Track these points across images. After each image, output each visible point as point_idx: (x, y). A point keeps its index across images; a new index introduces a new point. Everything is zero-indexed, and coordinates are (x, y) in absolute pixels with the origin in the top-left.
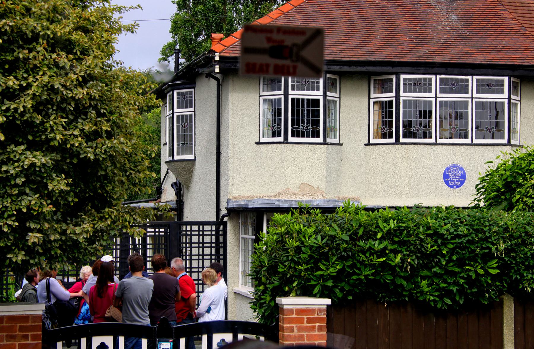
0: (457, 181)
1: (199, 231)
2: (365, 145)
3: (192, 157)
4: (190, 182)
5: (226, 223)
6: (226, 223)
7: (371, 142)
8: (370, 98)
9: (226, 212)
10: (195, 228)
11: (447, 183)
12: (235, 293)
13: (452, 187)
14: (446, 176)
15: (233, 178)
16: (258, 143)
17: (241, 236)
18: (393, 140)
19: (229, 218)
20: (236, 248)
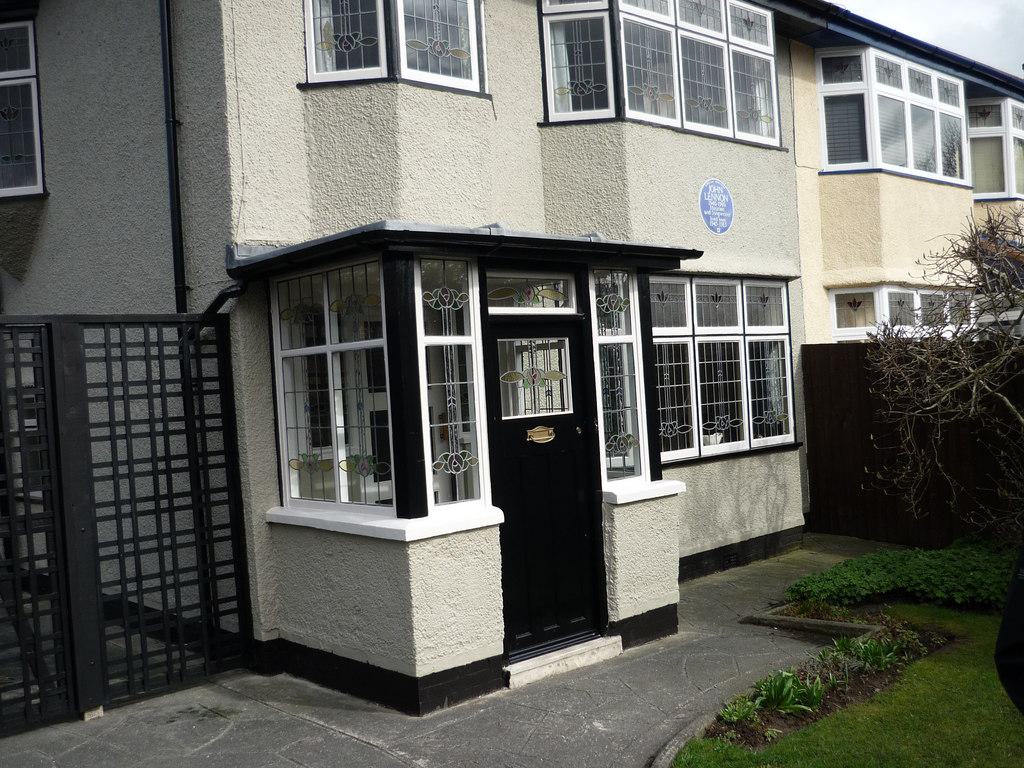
0: (722, 217)
1: (146, 344)
2: (539, 125)
3: (36, 189)
4: (27, 259)
5: (226, 317)
6: (226, 317)
7: (551, 119)
8: (540, 15)
9: (228, 282)
10: (134, 334)
11: (707, 218)
12: (270, 524)
13: (713, 229)
14: (705, 205)
15: (244, 182)
16: (304, 87)
17: (278, 355)
18: (610, 112)
19: (239, 302)
20: (268, 393)
